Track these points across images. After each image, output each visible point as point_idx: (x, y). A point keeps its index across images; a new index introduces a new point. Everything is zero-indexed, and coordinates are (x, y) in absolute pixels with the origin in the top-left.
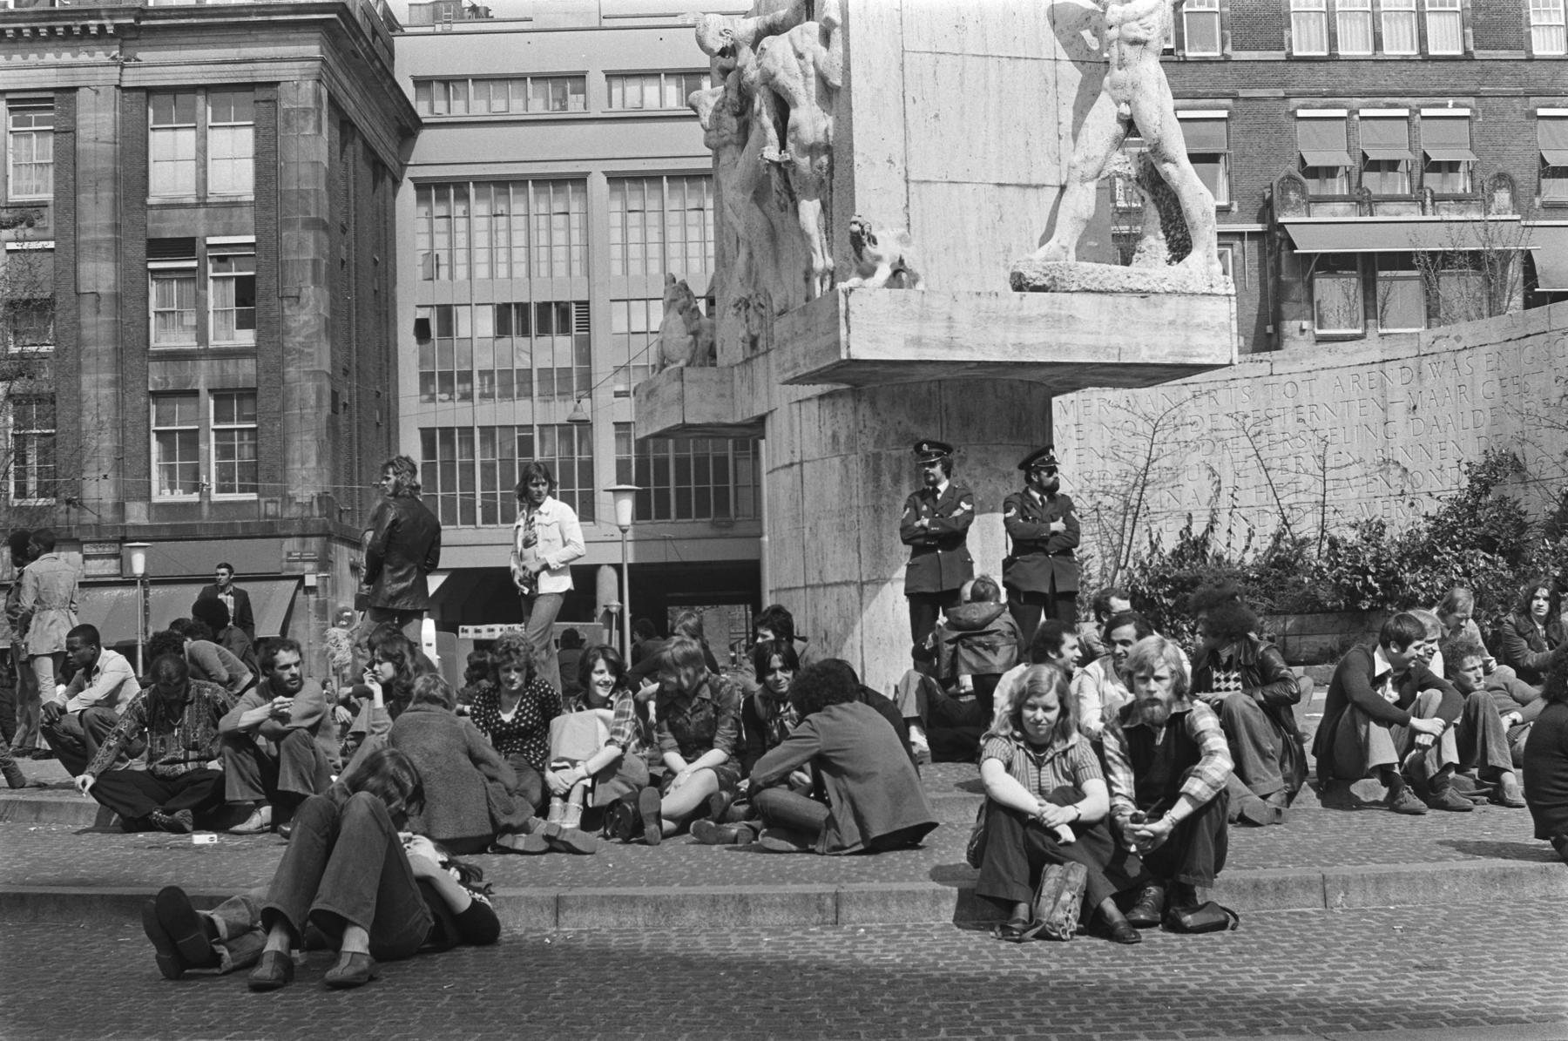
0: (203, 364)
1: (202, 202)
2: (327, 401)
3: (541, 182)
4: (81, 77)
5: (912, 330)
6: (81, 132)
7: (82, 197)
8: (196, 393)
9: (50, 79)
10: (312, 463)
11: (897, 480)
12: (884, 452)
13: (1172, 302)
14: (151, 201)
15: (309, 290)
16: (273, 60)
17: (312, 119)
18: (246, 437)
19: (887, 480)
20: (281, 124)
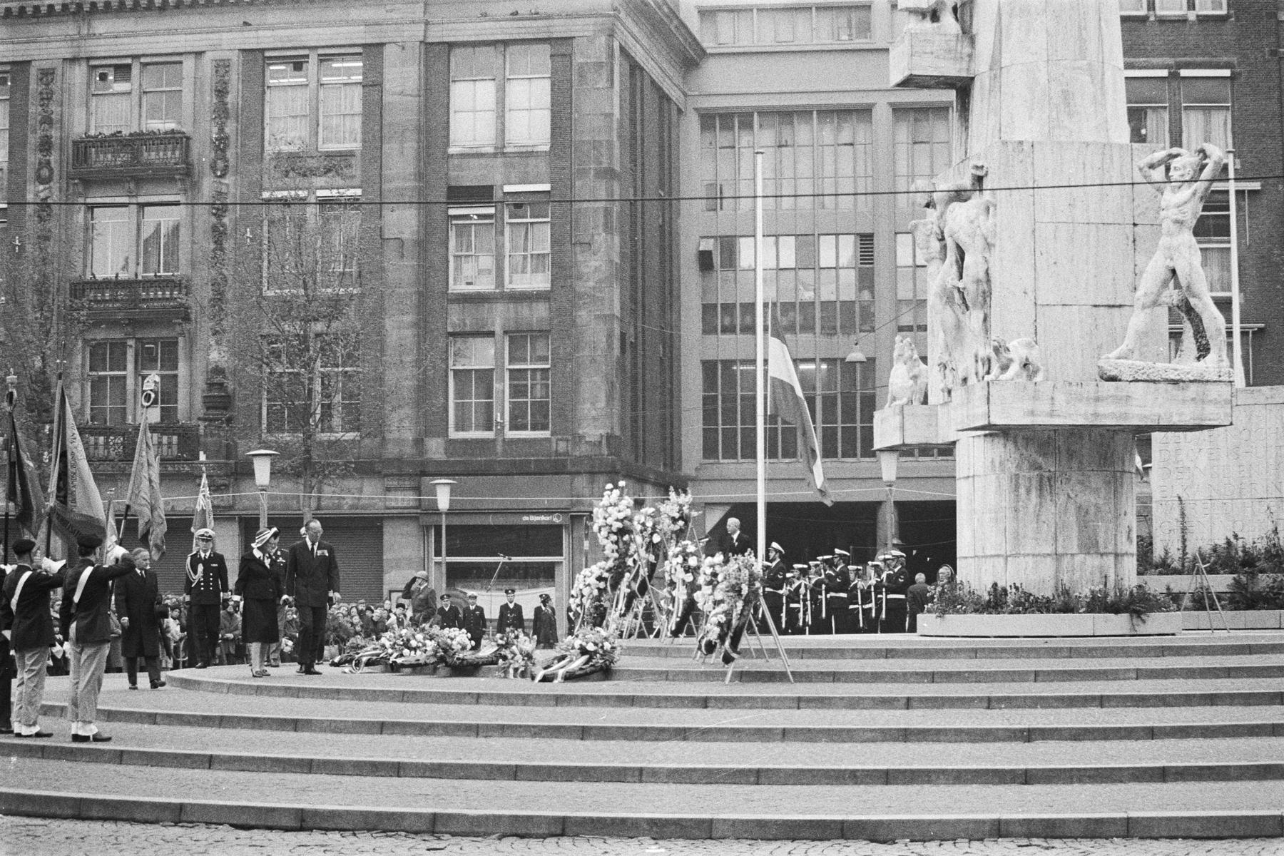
0: (500, 308)
1: (500, 152)
2: (617, 344)
3: (827, 113)
5: (1028, 405)
6: (387, 86)
7: (386, 147)
8: (491, 334)
9: (360, 35)
10: (602, 404)
11: (1028, 491)
12: (1022, 474)
13: (1193, 387)
14: (451, 150)
15: (601, 238)
18: (539, 375)
19: (1022, 491)
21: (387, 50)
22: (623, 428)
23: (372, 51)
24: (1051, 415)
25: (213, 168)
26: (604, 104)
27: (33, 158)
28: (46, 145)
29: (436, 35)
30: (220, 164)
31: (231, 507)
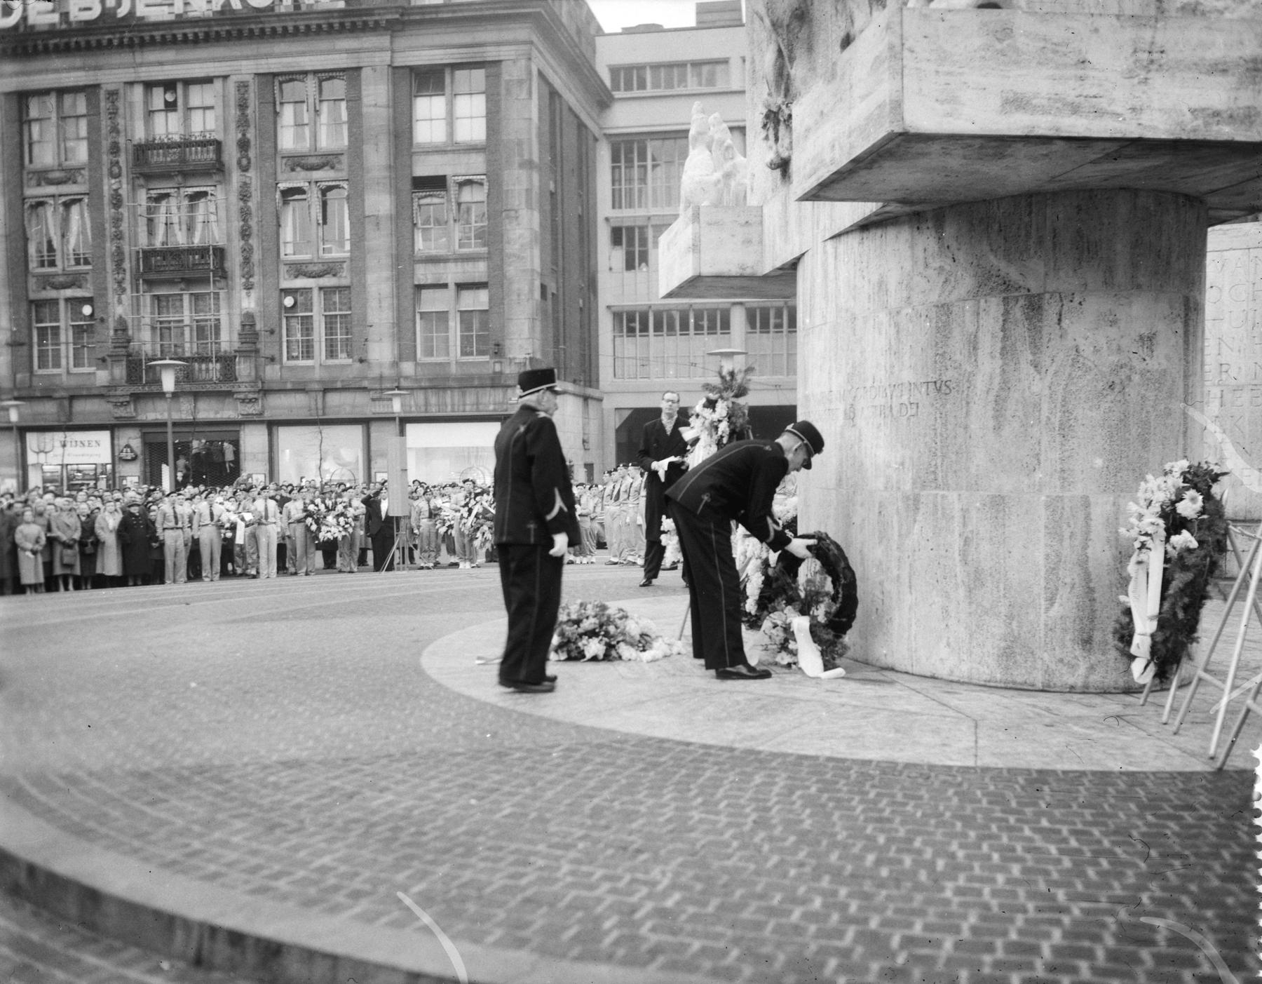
0: (451, 266)
4: (364, 60)
6: (365, 100)
7: (366, 148)
8: (445, 286)
9: (341, 61)
15: (524, 213)
16: (498, 44)
17: (525, 86)
20: (503, 92)
21: (364, 70)
22: (544, 353)
23: (352, 74)
24: (1075, 109)
25: (239, 163)
26: (526, 115)
27: (106, 159)
28: (115, 149)
29: (401, 60)
30: (244, 162)
31: (261, 414)
